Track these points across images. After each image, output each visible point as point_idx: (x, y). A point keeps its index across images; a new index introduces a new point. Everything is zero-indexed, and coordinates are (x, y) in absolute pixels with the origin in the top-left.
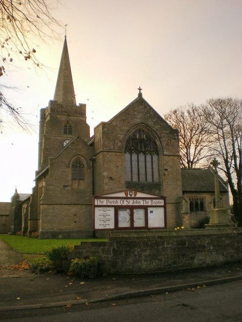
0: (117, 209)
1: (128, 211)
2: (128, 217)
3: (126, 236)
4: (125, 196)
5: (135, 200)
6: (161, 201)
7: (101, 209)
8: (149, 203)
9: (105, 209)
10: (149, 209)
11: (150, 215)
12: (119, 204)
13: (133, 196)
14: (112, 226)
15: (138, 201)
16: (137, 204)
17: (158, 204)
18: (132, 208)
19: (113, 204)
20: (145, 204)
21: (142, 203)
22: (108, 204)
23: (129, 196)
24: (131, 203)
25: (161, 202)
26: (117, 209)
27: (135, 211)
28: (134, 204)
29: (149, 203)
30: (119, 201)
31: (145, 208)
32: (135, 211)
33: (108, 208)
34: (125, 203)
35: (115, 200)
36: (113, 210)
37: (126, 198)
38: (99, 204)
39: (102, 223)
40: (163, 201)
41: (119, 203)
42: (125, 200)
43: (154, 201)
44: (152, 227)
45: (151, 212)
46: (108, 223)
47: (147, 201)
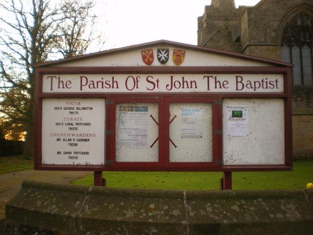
0: (114, 103)
1: (153, 111)
2: (152, 132)
3: (54, 209)
4: (142, 64)
5: (178, 78)
6: (272, 78)
7: (62, 103)
8: (231, 84)
9: (74, 104)
10: (228, 108)
11: (229, 125)
12: (122, 89)
13: (171, 63)
14: (97, 158)
15: (189, 78)
16: (186, 90)
17: (260, 90)
18: (164, 103)
19: (100, 90)
20: (213, 90)
21: (202, 85)
22: (86, 90)
23: (156, 63)
24: (163, 84)
25: (275, 83)
26: (114, 103)
27: (176, 111)
28: (174, 90)
29: (231, 84)
30: (121, 79)
31: (215, 102)
32: (176, 111)
33: (85, 103)
34: (144, 86)
35: (108, 78)
36: (98, 109)
37: (148, 71)
38: (56, 90)
39: (64, 146)
40: (280, 79)
41: (123, 85)
42: (142, 79)
43: (246, 78)
44: (237, 163)
45: (237, 115)
46: (82, 146)
47: (221, 78)
